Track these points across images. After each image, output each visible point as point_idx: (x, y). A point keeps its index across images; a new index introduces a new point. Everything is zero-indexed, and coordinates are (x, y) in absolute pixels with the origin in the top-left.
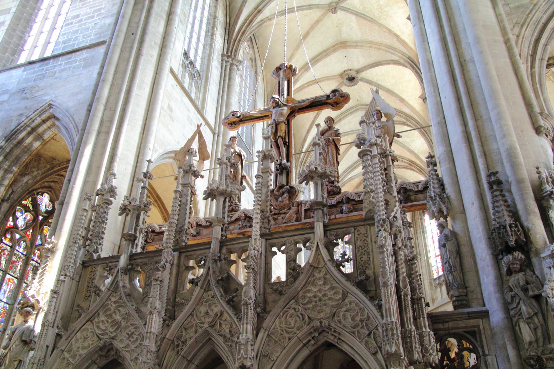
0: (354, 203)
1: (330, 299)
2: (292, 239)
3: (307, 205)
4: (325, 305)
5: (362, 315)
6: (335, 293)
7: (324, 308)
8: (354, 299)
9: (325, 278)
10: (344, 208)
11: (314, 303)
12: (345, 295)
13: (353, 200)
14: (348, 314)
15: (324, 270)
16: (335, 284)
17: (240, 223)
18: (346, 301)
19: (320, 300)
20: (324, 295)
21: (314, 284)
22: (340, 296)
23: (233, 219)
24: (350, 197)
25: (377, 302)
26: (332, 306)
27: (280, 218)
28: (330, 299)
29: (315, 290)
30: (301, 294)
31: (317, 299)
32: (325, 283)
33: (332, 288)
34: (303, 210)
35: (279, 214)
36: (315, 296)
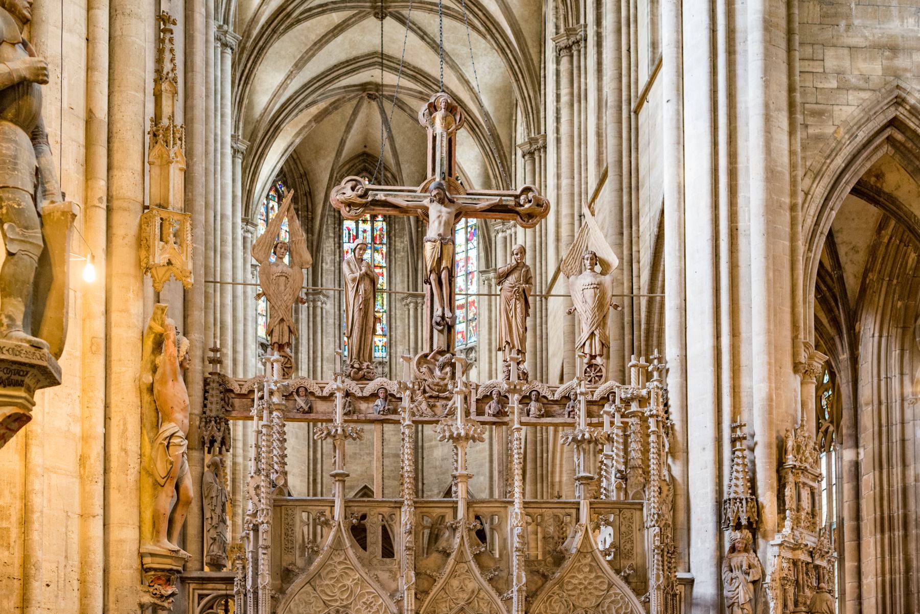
0: (545, 401)
1: (596, 588)
2: (550, 511)
3: (479, 391)
4: (590, 593)
5: (626, 609)
6: (601, 582)
7: (589, 596)
8: (618, 591)
9: (590, 565)
10: (533, 409)
11: (578, 591)
12: (611, 586)
13: (545, 397)
14: (613, 606)
15: (588, 556)
16: (600, 574)
17: (378, 402)
18: (611, 592)
19: (585, 588)
20: (590, 584)
21: (579, 570)
22: (606, 587)
23: (366, 393)
24: (540, 391)
25: (643, 599)
26: (598, 596)
27: (438, 404)
28: (596, 588)
29: (580, 576)
30: (566, 579)
31: (582, 587)
32: (590, 571)
33: (597, 577)
34: (473, 398)
35: (437, 397)
36: (580, 584)
